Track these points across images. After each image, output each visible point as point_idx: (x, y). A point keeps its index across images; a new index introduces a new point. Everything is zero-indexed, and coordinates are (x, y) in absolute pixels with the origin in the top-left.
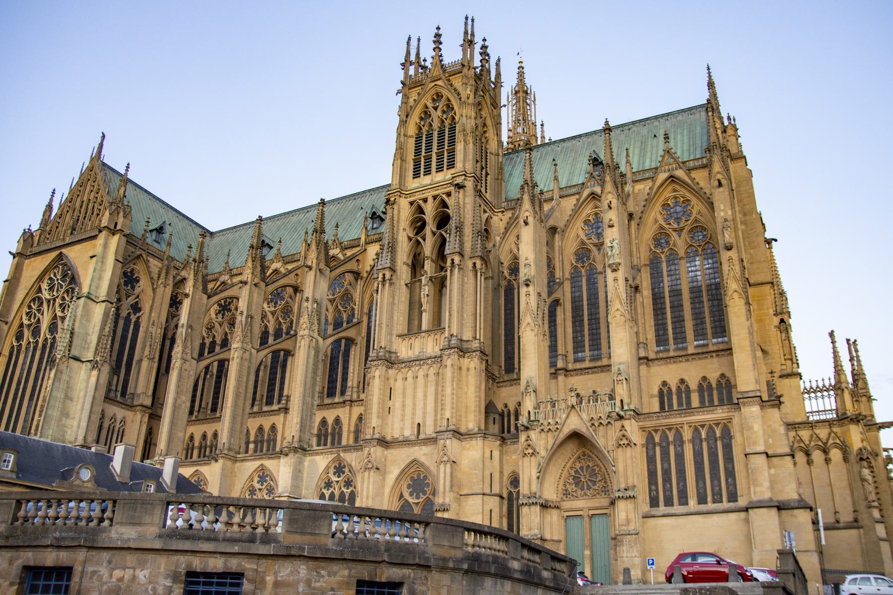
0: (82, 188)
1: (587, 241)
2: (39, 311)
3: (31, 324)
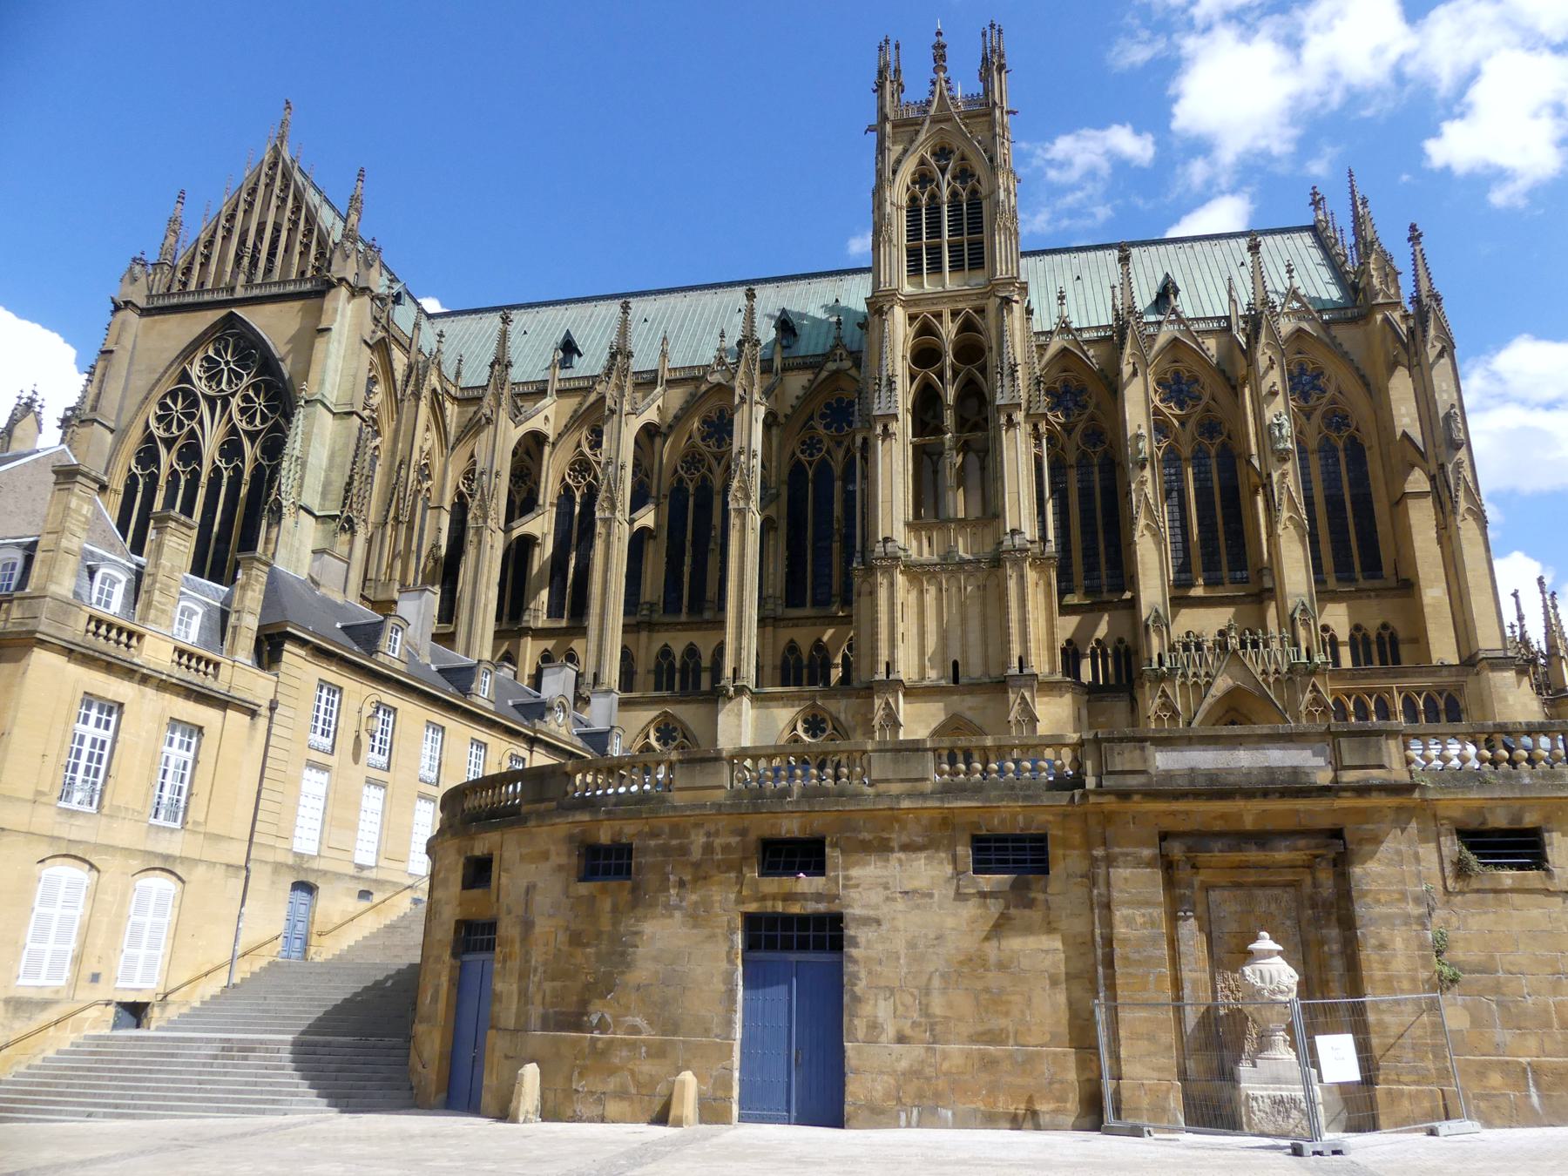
1: (1166, 411)
2: (191, 417)
3: (175, 439)
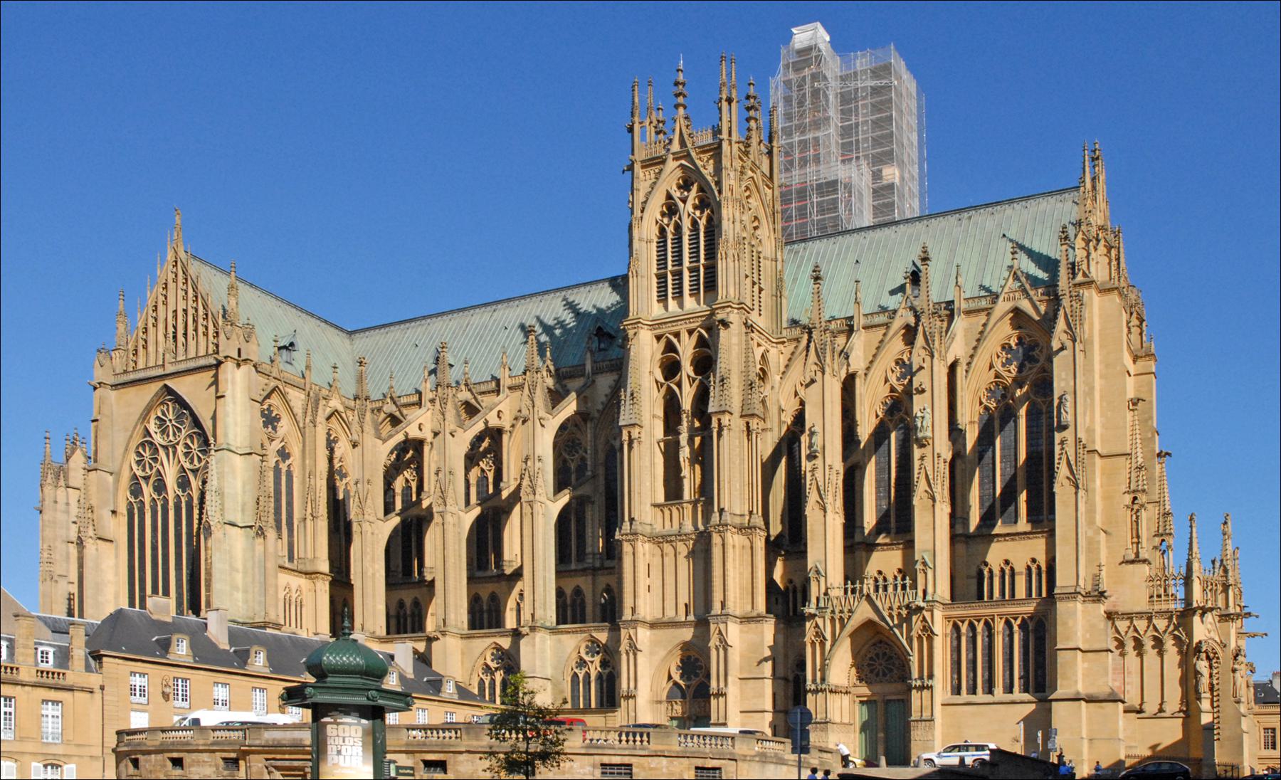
3: (149, 477)
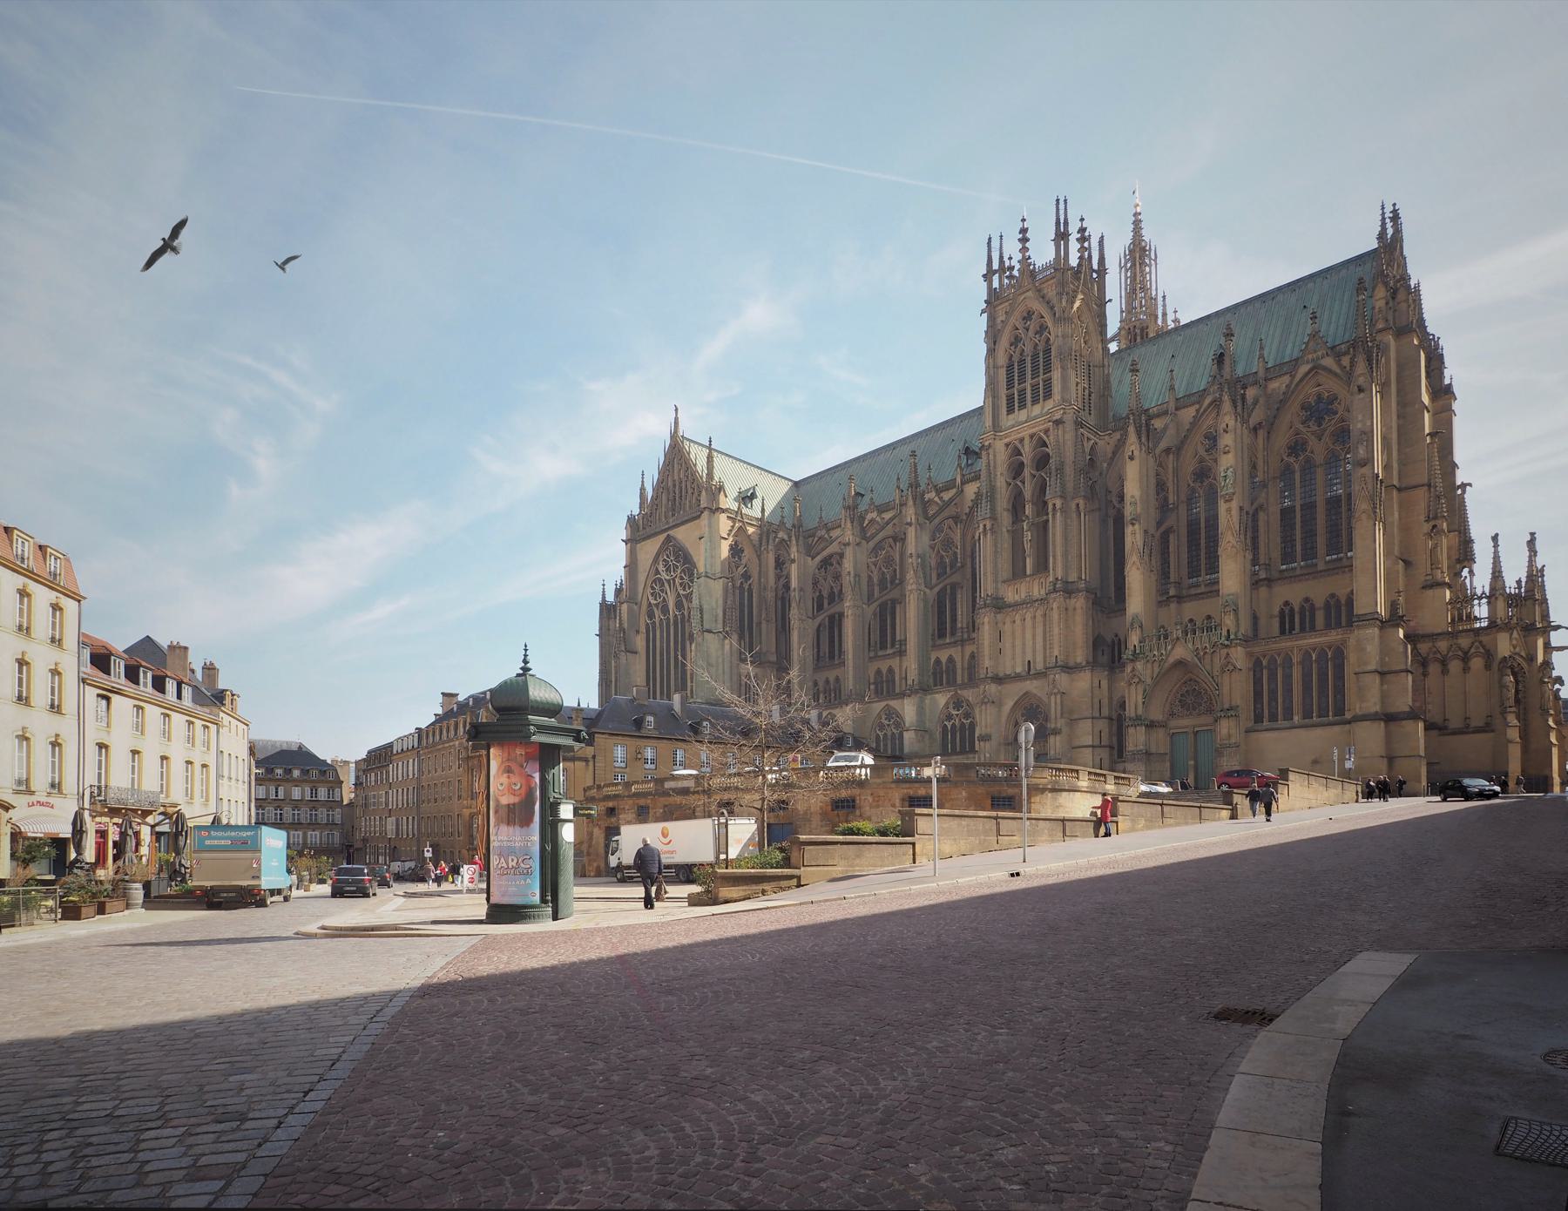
0: (670, 465)
2: (662, 591)
